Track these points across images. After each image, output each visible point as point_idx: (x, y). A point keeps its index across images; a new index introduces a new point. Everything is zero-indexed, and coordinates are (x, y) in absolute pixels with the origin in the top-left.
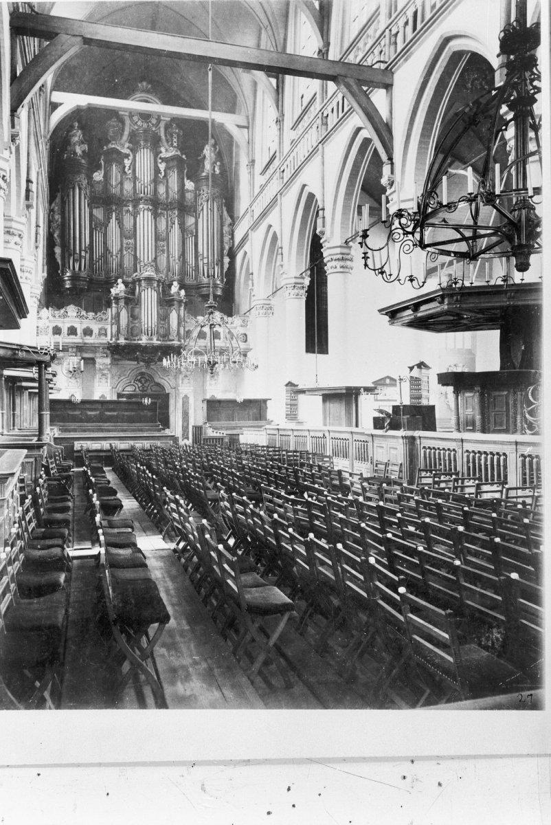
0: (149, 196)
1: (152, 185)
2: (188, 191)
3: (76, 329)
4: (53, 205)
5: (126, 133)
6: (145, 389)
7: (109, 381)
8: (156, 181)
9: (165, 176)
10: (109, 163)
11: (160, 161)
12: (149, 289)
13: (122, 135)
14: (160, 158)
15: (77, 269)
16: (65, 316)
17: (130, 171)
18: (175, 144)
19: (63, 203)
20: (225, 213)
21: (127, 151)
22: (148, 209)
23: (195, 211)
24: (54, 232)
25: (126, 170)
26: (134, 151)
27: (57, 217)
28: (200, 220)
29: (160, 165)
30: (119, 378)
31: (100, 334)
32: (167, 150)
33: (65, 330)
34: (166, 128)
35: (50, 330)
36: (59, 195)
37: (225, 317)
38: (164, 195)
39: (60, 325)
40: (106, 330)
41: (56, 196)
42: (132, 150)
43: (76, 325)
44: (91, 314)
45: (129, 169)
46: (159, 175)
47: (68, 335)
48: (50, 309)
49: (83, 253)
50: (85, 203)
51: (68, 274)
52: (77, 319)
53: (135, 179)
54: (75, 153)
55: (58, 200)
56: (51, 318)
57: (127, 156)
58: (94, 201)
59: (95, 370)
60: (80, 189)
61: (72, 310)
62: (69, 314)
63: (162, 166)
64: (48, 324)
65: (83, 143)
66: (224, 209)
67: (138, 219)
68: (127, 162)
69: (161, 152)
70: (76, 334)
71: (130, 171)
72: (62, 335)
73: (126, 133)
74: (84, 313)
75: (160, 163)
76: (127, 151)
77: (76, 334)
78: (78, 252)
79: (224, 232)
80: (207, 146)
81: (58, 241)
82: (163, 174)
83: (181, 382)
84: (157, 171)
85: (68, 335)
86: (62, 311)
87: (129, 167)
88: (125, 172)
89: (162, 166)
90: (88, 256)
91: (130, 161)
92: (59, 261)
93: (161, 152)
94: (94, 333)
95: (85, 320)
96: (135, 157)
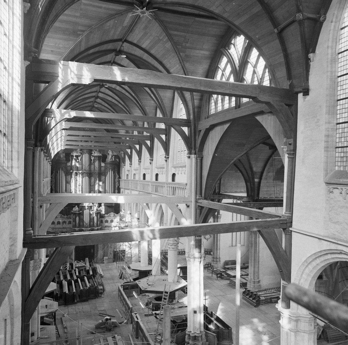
2: (102, 166)
4: (52, 176)
8: (90, 164)
9: (94, 162)
12: (87, 223)
20: (116, 174)
22: (87, 176)
23: (105, 174)
27: (54, 180)
28: (107, 177)
32: (94, 153)
37: (116, 214)
42: (81, 153)
50: (64, 175)
54: (60, 157)
55: (54, 174)
60: (62, 170)
65: (63, 153)
66: (116, 172)
69: (92, 153)
70: (60, 224)
71: (81, 161)
77: (60, 224)
79: (116, 181)
82: (93, 161)
84: (90, 160)
85: (57, 224)
89: (93, 158)
93: (92, 153)
96: (82, 156)
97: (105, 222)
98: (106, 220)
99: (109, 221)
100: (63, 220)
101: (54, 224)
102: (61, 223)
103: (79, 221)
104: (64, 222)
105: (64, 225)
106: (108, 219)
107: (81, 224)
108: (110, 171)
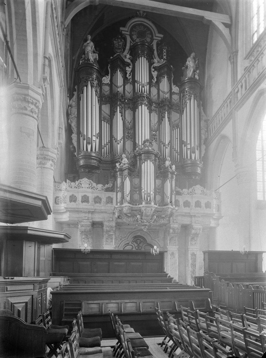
0: (145, 93)
1: (148, 86)
3: (88, 197)
5: (128, 47)
6: (141, 248)
7: (114, 241)
10: (114, 72)
11: (153, 70)
13: (124, 50)
14: (153, 68)
15: (89, 150)
16: (79, 187)
17: (131, 77)
18: (165, 57)
19: (79, 99)
21: (129, 61)
24: (72, 122)
25: (128, 76)
26: (134, 61)
27: (74, 111)
29: (153, 73)
30: (121, 239)
31: (107, 202)
33: (79, 199)
34: (158, 45)
35: (68, 199)
36: (75, 93)
38: (156, 96)
39: (76, 194)
40: (112, 199)
41: (74, 95)
42: (132, 61)
43: (88, 195)
44: (100, 186)
45: (130, 75)
46: (153, 80)
47: (82, 202)
48: (68, 181)
49: (94, 138)
50: (95, 99)
51: (82, 154)
52: (90, 190)
53: (134, 82)
56: (69, 189)
57: (128, 65)
58: (102, 99)
59: (103, 232)
61: (85, 182)
62: (83, 185)
63: (155, 74)
64: (66, 194)
67: (137, 113)
68: (129, 70)
72: (77, 203)
73: (128, 47)
74: (94, 184)
75: (154, 72)
76: (129, 61)
78: (90, 136)
80: (189, 58)
81: (75, 130)
83: (169, 242)
85: (82, 202)
86: (77, 182)
87: (130, 73)
88: (127, 78)
90: (98, 141)
91: (130, 69)
92: (75, 144)
94: (102, 201)
95: (96, 191)
97: (185, 206)
98: (187, 201)
99: (193, 204)
100: (96, 195)
101: (75, 201)
102: (91, 200)
103: (131, 191)
104: (97, 200)
105: (98, 206)
106: (190, 200)
107: (136, 197)
108: (190, 99)
